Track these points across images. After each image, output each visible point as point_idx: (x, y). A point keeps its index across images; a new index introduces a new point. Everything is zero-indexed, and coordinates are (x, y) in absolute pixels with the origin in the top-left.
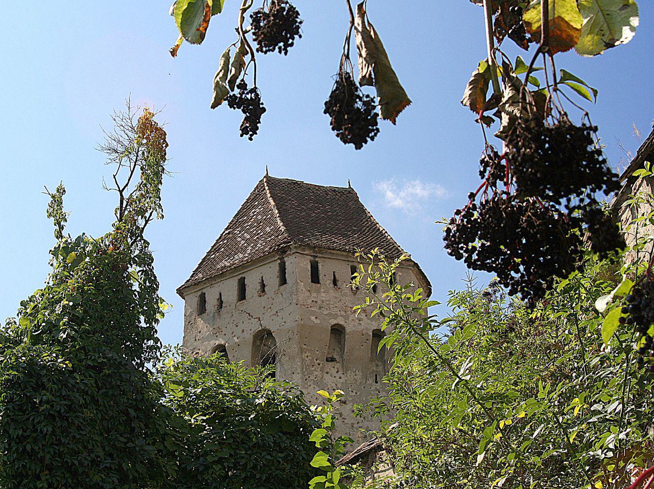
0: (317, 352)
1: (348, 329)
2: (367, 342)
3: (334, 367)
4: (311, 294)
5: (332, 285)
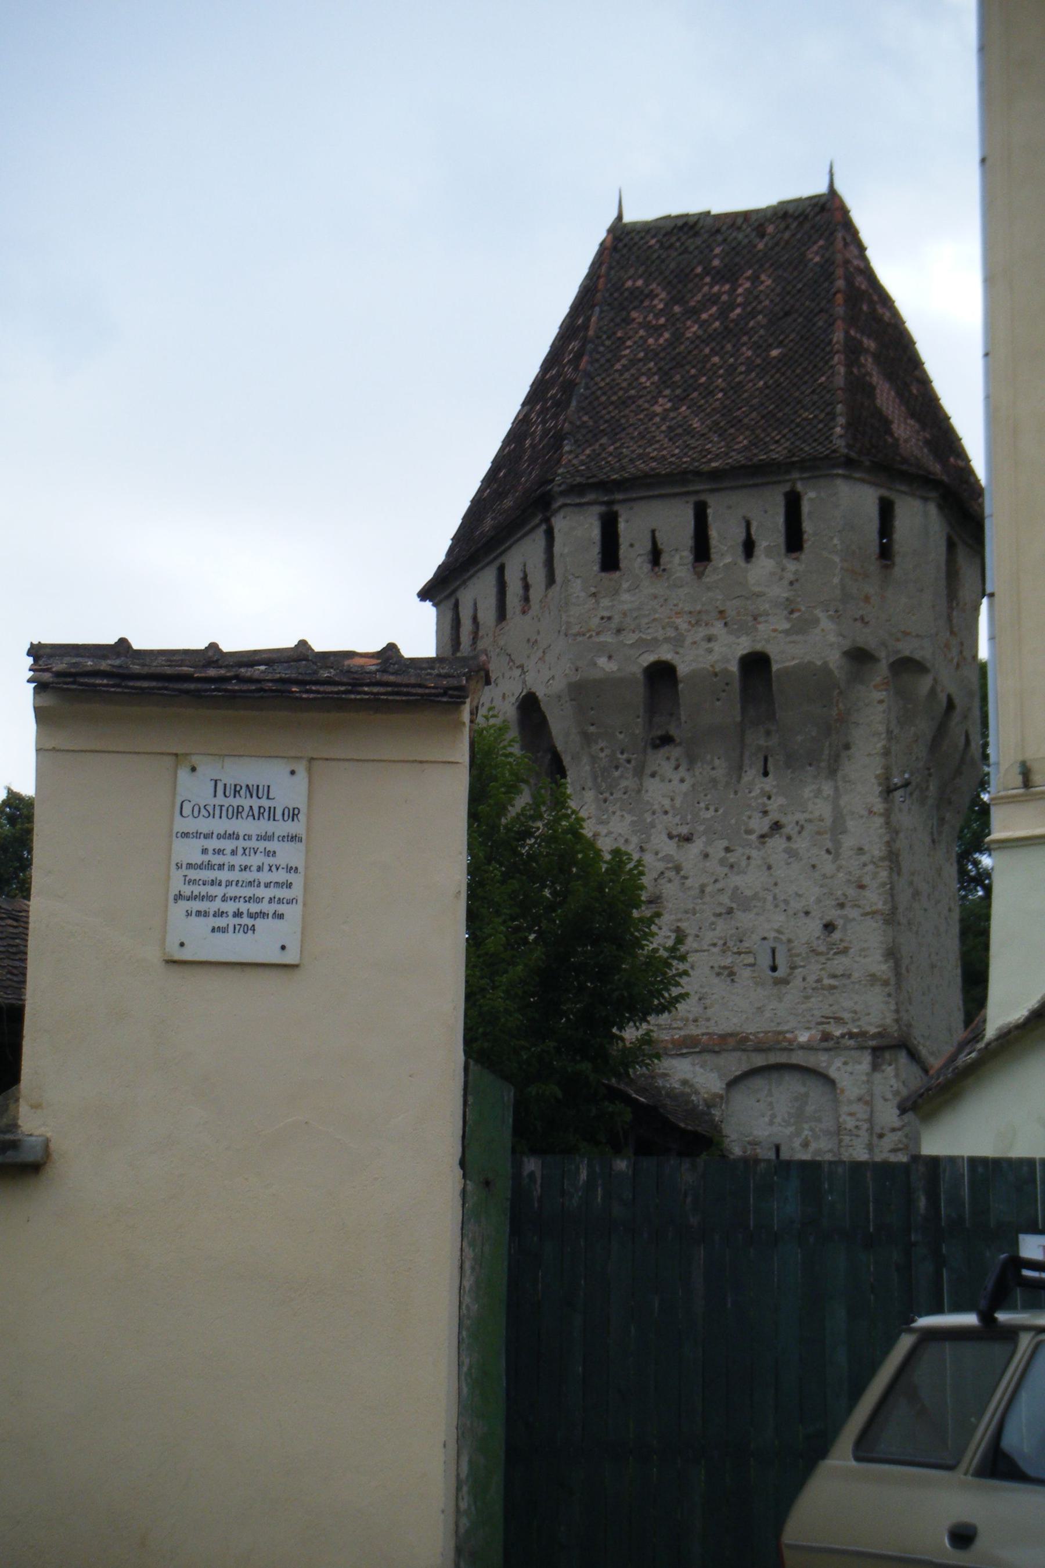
0: (621, 737)
1: (682, 670)
2: (727, 688)
3: (668, 758)
4: (597, 602)
5: (648, 566)
